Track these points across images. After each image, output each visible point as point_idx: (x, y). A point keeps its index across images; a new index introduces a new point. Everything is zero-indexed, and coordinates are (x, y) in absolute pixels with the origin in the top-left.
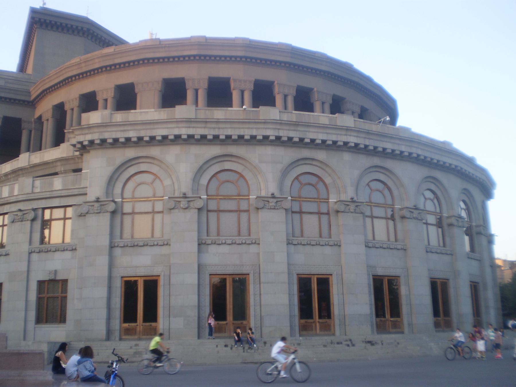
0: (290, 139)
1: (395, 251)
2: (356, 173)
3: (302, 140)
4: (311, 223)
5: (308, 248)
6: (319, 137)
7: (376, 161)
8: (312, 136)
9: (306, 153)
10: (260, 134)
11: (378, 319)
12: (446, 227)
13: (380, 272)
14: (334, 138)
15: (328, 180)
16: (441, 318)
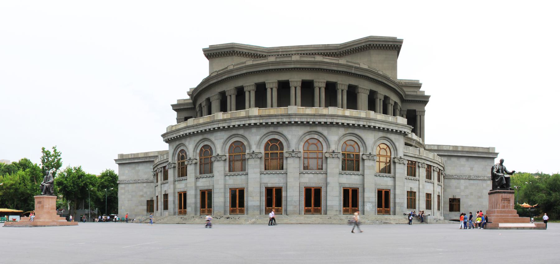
0: (224, 127)
1: (281, 175)
2: (258, 138)
3: (229, 127)
4: (238, 164)
5: (235, 176)
6: (237, 123)
7: (272, 129)
8: (233, 124)
9: (234, 132)
10: (211, 127)
11: (267, 208)
12: (324, 158)
13: (270, 185)
14: (243, 123)
15: (245, 143)
16: (312, 208)
